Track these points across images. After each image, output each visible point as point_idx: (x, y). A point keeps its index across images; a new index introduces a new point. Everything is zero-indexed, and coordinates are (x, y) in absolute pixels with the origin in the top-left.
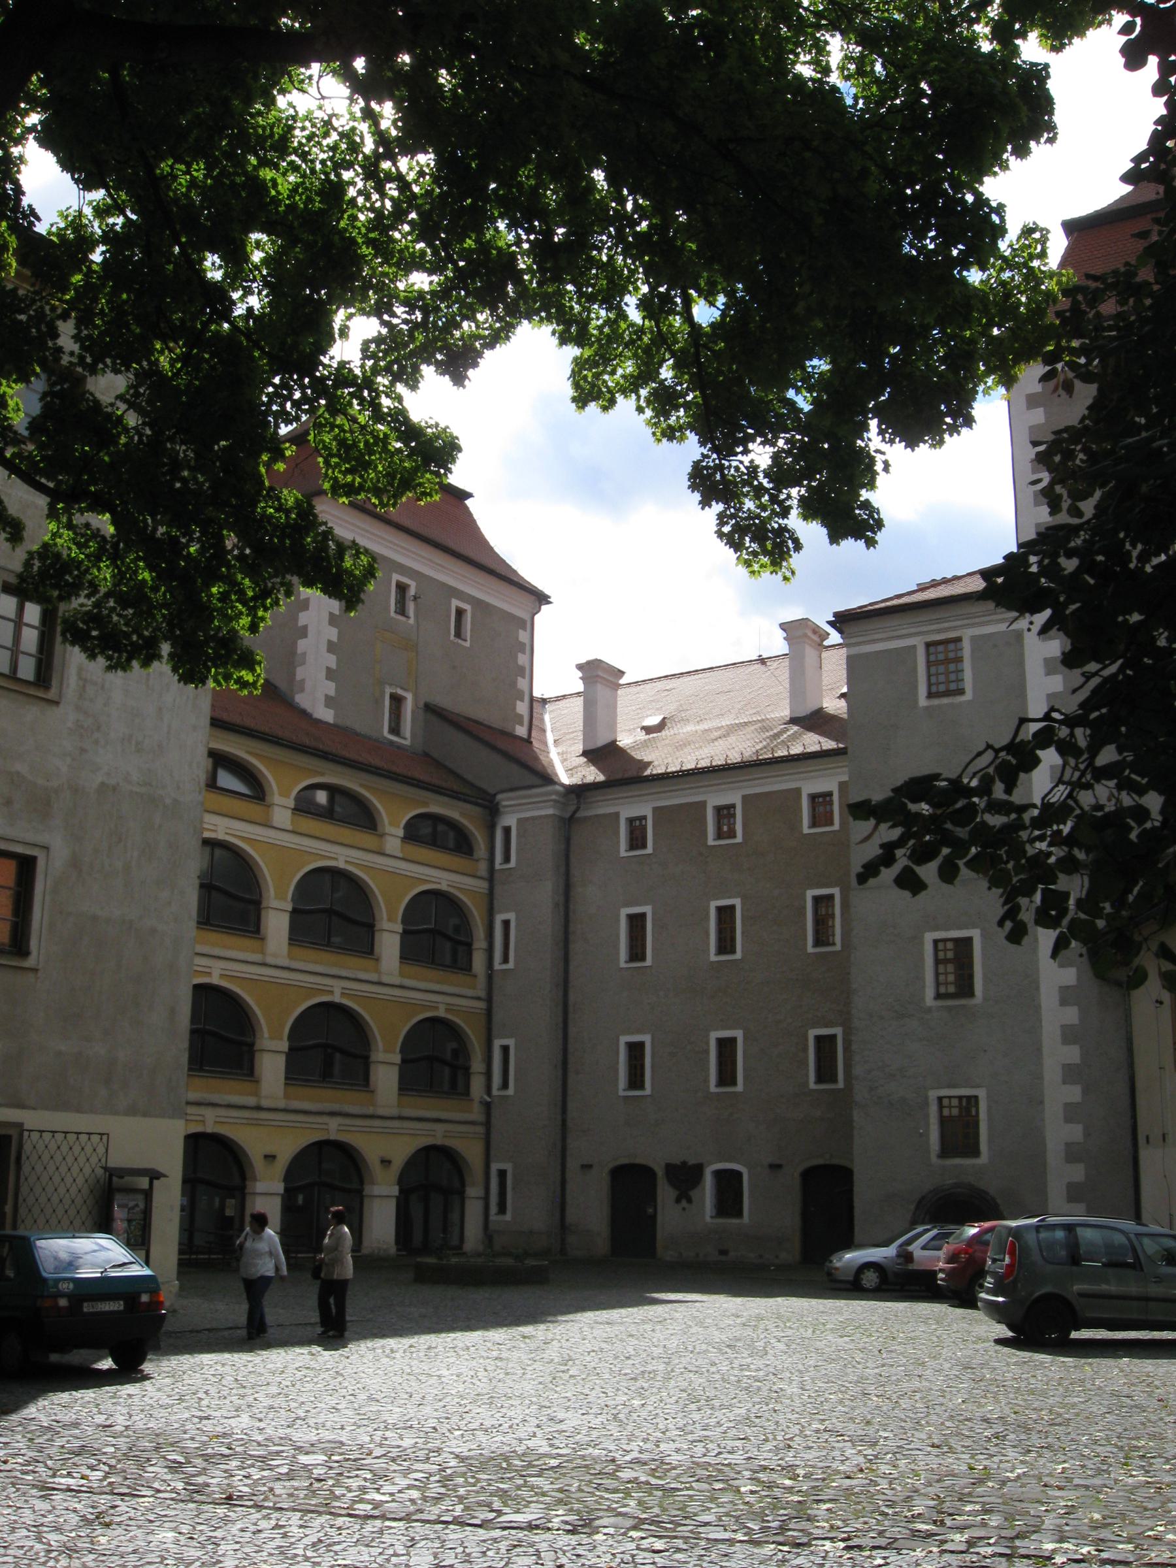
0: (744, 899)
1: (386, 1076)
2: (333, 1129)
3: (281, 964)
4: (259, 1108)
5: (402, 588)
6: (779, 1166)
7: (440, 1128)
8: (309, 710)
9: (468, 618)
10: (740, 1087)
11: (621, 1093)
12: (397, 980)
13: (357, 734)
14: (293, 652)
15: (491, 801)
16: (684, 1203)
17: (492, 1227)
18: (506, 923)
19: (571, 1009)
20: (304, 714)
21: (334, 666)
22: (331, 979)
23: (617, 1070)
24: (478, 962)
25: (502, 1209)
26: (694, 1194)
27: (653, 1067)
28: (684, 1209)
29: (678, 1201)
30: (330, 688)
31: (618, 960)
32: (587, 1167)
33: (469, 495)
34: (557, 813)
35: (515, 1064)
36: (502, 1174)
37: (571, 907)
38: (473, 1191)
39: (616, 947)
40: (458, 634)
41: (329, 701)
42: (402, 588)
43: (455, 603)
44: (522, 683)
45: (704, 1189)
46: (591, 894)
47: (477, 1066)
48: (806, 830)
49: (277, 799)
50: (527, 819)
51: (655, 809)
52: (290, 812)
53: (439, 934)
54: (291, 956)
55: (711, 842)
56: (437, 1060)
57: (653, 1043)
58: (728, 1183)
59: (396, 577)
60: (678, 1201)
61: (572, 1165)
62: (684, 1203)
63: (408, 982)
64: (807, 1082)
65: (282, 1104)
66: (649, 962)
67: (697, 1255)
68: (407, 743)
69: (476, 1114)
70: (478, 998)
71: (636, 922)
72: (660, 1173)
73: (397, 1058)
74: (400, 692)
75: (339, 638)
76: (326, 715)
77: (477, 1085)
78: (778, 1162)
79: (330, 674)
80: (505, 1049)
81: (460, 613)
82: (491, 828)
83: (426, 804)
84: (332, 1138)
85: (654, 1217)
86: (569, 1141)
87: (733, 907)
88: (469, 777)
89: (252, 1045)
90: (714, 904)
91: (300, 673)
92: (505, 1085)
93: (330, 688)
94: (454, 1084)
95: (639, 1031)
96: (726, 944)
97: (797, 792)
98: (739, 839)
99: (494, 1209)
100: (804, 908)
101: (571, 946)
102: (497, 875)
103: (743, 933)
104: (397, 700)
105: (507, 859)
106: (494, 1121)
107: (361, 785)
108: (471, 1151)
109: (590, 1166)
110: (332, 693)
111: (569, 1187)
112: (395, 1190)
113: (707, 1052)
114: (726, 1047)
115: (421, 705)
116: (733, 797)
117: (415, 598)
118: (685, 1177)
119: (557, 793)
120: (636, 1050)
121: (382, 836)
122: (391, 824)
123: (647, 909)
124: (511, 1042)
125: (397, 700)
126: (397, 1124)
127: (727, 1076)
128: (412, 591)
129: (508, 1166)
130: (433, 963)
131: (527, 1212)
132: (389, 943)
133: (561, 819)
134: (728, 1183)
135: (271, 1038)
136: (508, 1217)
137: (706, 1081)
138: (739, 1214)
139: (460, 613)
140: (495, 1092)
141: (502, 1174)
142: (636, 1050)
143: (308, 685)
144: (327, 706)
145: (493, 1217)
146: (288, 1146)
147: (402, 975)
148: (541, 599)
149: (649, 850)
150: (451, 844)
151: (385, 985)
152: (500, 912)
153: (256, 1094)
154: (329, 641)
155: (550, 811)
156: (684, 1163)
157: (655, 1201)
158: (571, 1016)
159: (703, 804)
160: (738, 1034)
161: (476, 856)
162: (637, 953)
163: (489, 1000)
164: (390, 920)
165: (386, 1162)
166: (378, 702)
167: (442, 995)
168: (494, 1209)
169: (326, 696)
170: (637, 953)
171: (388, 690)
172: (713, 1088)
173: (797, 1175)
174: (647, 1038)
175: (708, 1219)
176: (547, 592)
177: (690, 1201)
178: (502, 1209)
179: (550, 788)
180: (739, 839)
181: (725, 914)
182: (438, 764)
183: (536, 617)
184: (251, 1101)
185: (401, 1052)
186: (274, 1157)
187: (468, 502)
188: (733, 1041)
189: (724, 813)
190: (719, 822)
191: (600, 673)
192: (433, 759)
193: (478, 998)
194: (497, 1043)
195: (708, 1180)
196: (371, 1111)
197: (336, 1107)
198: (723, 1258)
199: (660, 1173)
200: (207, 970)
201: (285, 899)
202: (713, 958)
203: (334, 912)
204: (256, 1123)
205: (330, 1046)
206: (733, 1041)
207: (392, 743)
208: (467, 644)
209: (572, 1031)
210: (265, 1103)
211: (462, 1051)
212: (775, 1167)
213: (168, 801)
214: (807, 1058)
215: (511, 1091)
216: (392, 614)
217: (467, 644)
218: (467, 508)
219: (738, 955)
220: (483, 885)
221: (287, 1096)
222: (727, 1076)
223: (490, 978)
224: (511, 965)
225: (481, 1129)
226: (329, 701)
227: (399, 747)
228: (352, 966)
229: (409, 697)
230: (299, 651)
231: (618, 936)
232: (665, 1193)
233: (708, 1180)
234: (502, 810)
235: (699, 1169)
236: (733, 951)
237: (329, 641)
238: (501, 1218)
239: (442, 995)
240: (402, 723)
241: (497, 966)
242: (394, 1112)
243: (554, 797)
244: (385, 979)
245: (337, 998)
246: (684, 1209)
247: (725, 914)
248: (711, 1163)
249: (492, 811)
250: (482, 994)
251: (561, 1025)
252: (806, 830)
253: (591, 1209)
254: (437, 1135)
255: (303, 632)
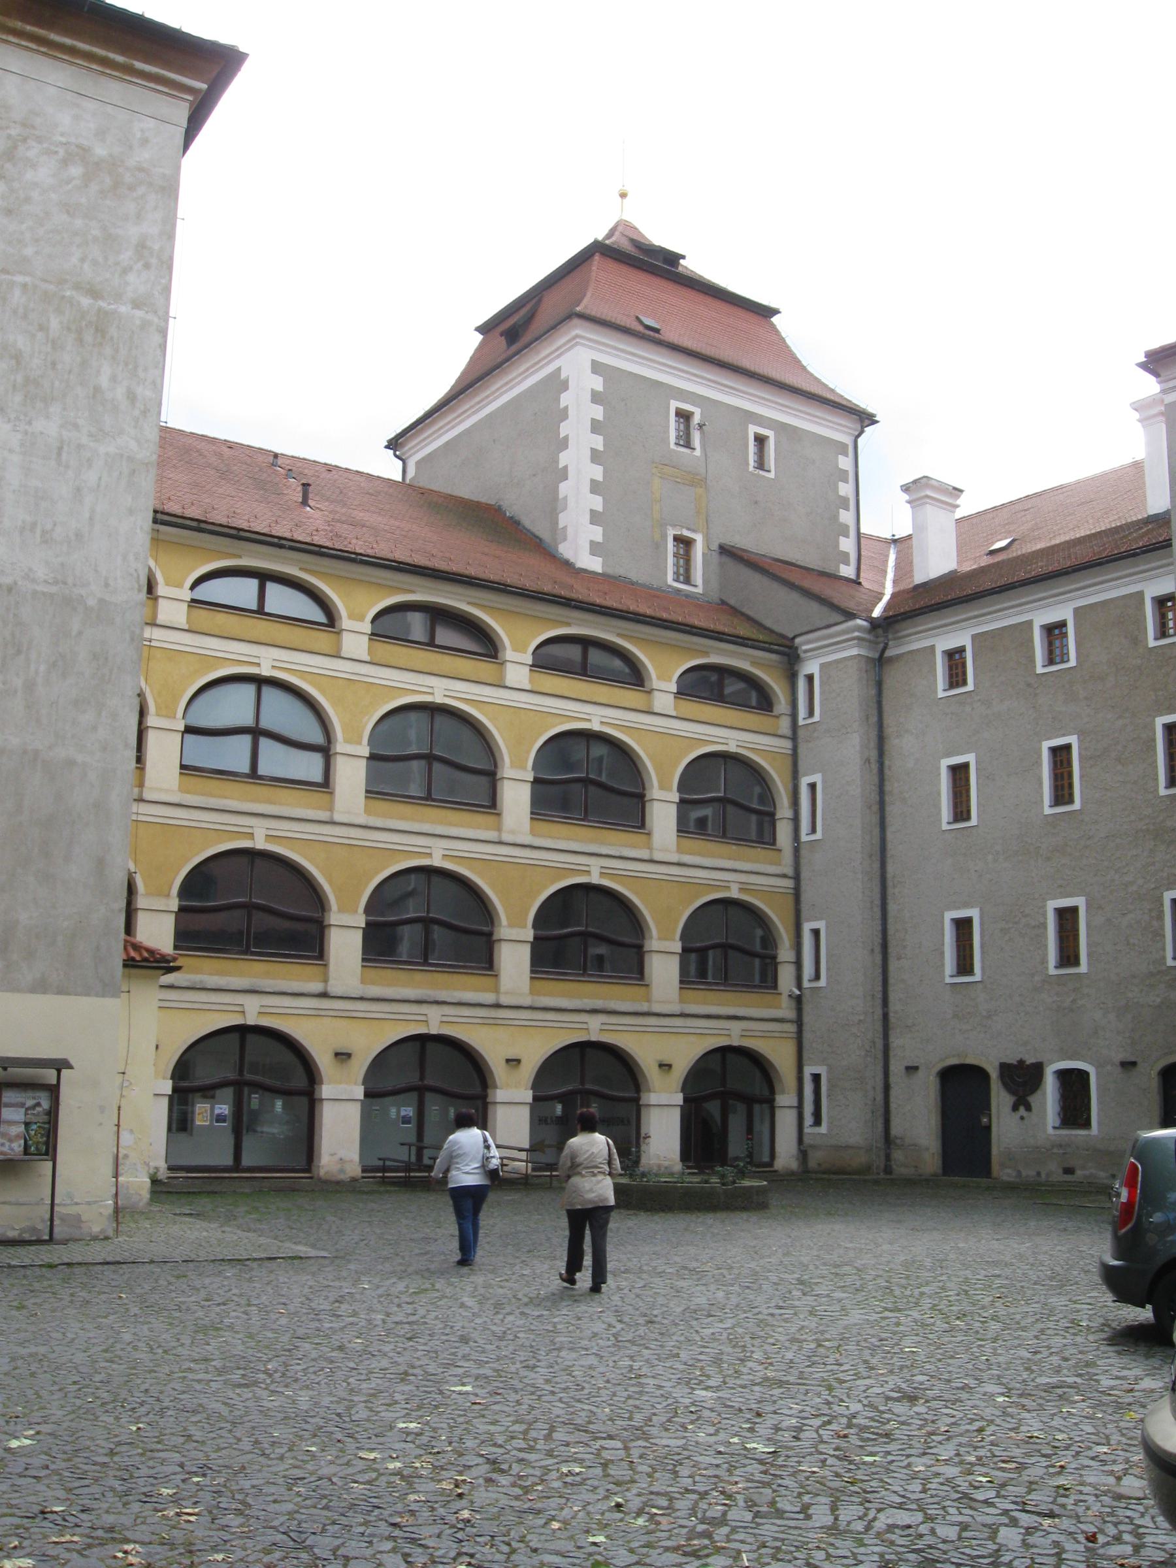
0: (1082, 734)
1: (664, 967)
2: (595, 1029)
3: (519, 841)
4: (498, 1006)
5: (684, 417)
6: (1134, 1064)
7: (736, 1027)
8: (572, 560)
9: (771, 445)
10: (1083, 968)
11: (948, 980)
12: (674, 858)
13: (633, 583)
14: (555, 498)
15: (790, 647)
16: (1022, 1109)
17: (806, 1140)
18: (813, 786)
19: (890, 883)
20: (567, 564)
21: (600, 508)
22: (589, 856)
23: (942, 953)
24: (783, 833)
25: (818, 1121)
26: (1033, 1100)
27: (982, 946)
28: (1022, 1118)
29: (1015, 1108)
30: (597, 533)
31: (940, 820)
32: (911, 1069)
33: (775, 312)
34: (863, 652)
35: (827, 952)
36: (816, 1078)
37: (887, 763)
38: (785, 1099)
39: (937, 806)
40: (761, 464)
41: (595, 549)
42: (684, 417)
43: (753, 429)
44: (846, 517)
45: (1044, 1094)
46: (906, 746)
47: (785, 954)
48: (1152, 643)
49: (509, 654)
50: (830, 663)
51: (974, 637)
52: (528, 668)
53: (728, 799)
54: (533, 832)
55: (1040, 670)
56: (730, 948)
57: (982, 918)
58: (1074, 1085)
59: (674, 405)
60: (1015, 1108)
61: (896, 1067)
62: (1022, 1109)
63: (687, 859)
64: (1164, 958)
65: (527, 1001)
66: (974, 821)
67: (1039, 1174)
68: (699, 590)
69: (786, 1010)
70: (784, 876)
71: (959, 773)
72: (994, 1075)
73: (677, 947)
74: (686, 533)
75: (604, 477)
76: (595, 564)
77: (786, 977)
78: (1133, 1059)
79: (595, 518)
80: (816, 933)
81: (760, 440)
82: (792, 677)
83: (706, 654)
84: (593, 1039)
85: (988, 1128)
86: (891, 1040)
87: (1068, 747)
88: (768, 623)
89: (491, 934)
90: (1046, 745)
91: (563, 519)
92: (817, 977)
93: (597, 533)
94: (763, 978)
95: (966, 905)
96: (1062, 794)
97: (1141, 594)
98: (1073, 662)
99: (808, 1119)
100: (1154, 740)
101: (888, 809)
102: (801, 733)
103: (1082, 777)
104: (684, 543)
105: (811, 713)
106: (806, 1019)
107: (619, 635)
108: (780, 1055)
109: (916, 1068)
110: (599, 538)
111: (894, 1093)
112: (679, 1099)
113: (1044, 926)
114: (1067, 916)
115: (715, 547)
116: (1063, 612)
117: (701, 426)
118: (1023, 1079)
119: (859, 628)
120: (963, 926)
121: (650, 692)
122: (659, 678)
123: (970, 758)
124: (820, 925)
125: (684, 543)
126: (678, 1022)
127: (1068, 956)
128: (696, 419)
129: (821, 1070)
130: (724, 836)
131: (846, 1126)
132: (663, 814)
133: (873, 660)
134: (1074, 1085)
135: (511, 925)
136: (823, 1129)
137: (1044, 961)
138: (1087, 1124)
139: (760, 440)
140: (806, 984)
141: (816, 1078)
142: (963, 926)
143: (570, 532)
144: (593, 553)
145: (807, 1130)
146: (536, 1049)
147: (680, 850)
148: (865, 419)
149: (970, 686)
150: (754, 703)
151: (661, 865)
152: (806, 775)
153: (497, 990)
154: (592, 481)
155: (855, 652)
156: (1021, 1062)
157: (988, 1106)
158: (890, 891)
159: (1029, 623)
160: (1079, 902)
161: (775, 713)
162: (961, 812)
163: (797, 877)
164: (662, 788)
165: (665, 1067)
166: (659, 546)
167: (733, 872)
168: (808, 1119)
169: (592, 542)
170: (961, 812)
171: (671, 532)
172: (1052, 971)
173: (1154, 1074)
174: (974, 913)
175: (1050, 1131)
176: (870, 410)
177: (1028, 1108)
178: (818, 1121)
179: (851, 624)
180: (1073, 662)
181: (1061, 754)
182: (735, 612)
183: (859, 440)
184: (489, 998)
185: (681, 939)
186: (518, 1061)
187: (775, 320)
188: (1074, 910)
189: (1055, 631)
190: (1050, 644)
191: (929, 493)
192: (732, 607)
193: (784, 876)
194: (807, 927)
195: (1050, 1086)
196: (644, 1007)
197: (599, 1004)
198: (1068, 1178)
199: (994, 1075)
200: (428, 851)
201: (524, 768)
202: (1048, 811)
203: (589, 781)
204: (495, 1023)
205: (587, 933)
206: (1074, 910)
207: (679, 591)
208: (772, 475)
209: (892, 907)
210: (504, 1000)
211: (769, 940)
212: (1128, 1065)
213: (91, 602)
214: (1162, 927)
215: (822, 982)
216: (672, 446)
217: (772, 475)
218: (773, 326)
219: (1077, 805)
220: (788, 744)
221: (532, 992)
222: (1068, 956)
223: (797, 851)
224: (818, 835)
225: (792, 1028)
226: (595, 549)
227: (688, 595)
228: (616, 842)
229: (699, 538)
230: (561, 496)
231: (939, 794)
232: (1000, 1098)
233: (1050, 1086)
234: (802, 655)
235: (1037, 1070)
236: (1071, 801)
237: (592, 481)
238: (816, 1130)
239: (733, 872)
240: (692, 571)
241: (804, 838)
242: (676, 1008)
243: (856, 634)
244: (658, 856)
245: (595, 879)
246: (1022, 1118)
247: (1061, 754)
248: (1051, 1062)
249: (789, 656)
250: (789, 871)
251: (878, 902)
252: (1152, 643)
253: (919, 1120)
254: (734, 1035)
255: (563, 474)
